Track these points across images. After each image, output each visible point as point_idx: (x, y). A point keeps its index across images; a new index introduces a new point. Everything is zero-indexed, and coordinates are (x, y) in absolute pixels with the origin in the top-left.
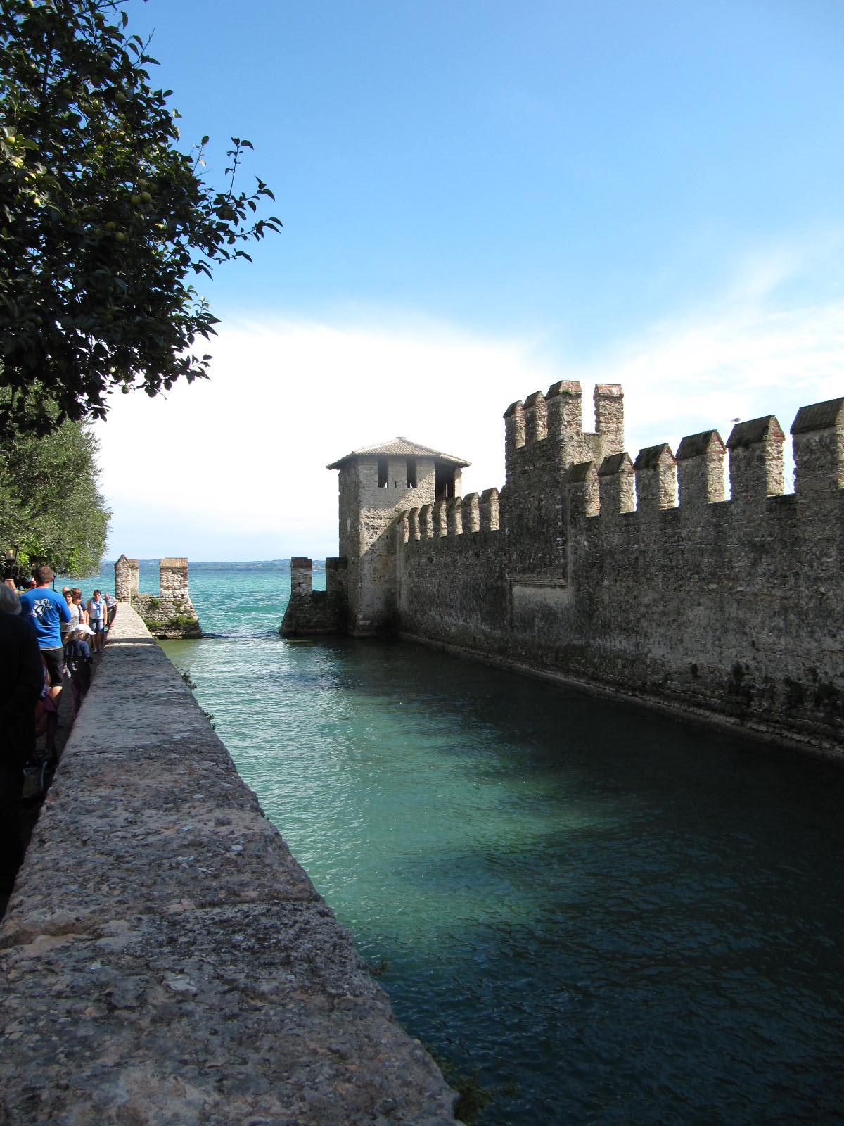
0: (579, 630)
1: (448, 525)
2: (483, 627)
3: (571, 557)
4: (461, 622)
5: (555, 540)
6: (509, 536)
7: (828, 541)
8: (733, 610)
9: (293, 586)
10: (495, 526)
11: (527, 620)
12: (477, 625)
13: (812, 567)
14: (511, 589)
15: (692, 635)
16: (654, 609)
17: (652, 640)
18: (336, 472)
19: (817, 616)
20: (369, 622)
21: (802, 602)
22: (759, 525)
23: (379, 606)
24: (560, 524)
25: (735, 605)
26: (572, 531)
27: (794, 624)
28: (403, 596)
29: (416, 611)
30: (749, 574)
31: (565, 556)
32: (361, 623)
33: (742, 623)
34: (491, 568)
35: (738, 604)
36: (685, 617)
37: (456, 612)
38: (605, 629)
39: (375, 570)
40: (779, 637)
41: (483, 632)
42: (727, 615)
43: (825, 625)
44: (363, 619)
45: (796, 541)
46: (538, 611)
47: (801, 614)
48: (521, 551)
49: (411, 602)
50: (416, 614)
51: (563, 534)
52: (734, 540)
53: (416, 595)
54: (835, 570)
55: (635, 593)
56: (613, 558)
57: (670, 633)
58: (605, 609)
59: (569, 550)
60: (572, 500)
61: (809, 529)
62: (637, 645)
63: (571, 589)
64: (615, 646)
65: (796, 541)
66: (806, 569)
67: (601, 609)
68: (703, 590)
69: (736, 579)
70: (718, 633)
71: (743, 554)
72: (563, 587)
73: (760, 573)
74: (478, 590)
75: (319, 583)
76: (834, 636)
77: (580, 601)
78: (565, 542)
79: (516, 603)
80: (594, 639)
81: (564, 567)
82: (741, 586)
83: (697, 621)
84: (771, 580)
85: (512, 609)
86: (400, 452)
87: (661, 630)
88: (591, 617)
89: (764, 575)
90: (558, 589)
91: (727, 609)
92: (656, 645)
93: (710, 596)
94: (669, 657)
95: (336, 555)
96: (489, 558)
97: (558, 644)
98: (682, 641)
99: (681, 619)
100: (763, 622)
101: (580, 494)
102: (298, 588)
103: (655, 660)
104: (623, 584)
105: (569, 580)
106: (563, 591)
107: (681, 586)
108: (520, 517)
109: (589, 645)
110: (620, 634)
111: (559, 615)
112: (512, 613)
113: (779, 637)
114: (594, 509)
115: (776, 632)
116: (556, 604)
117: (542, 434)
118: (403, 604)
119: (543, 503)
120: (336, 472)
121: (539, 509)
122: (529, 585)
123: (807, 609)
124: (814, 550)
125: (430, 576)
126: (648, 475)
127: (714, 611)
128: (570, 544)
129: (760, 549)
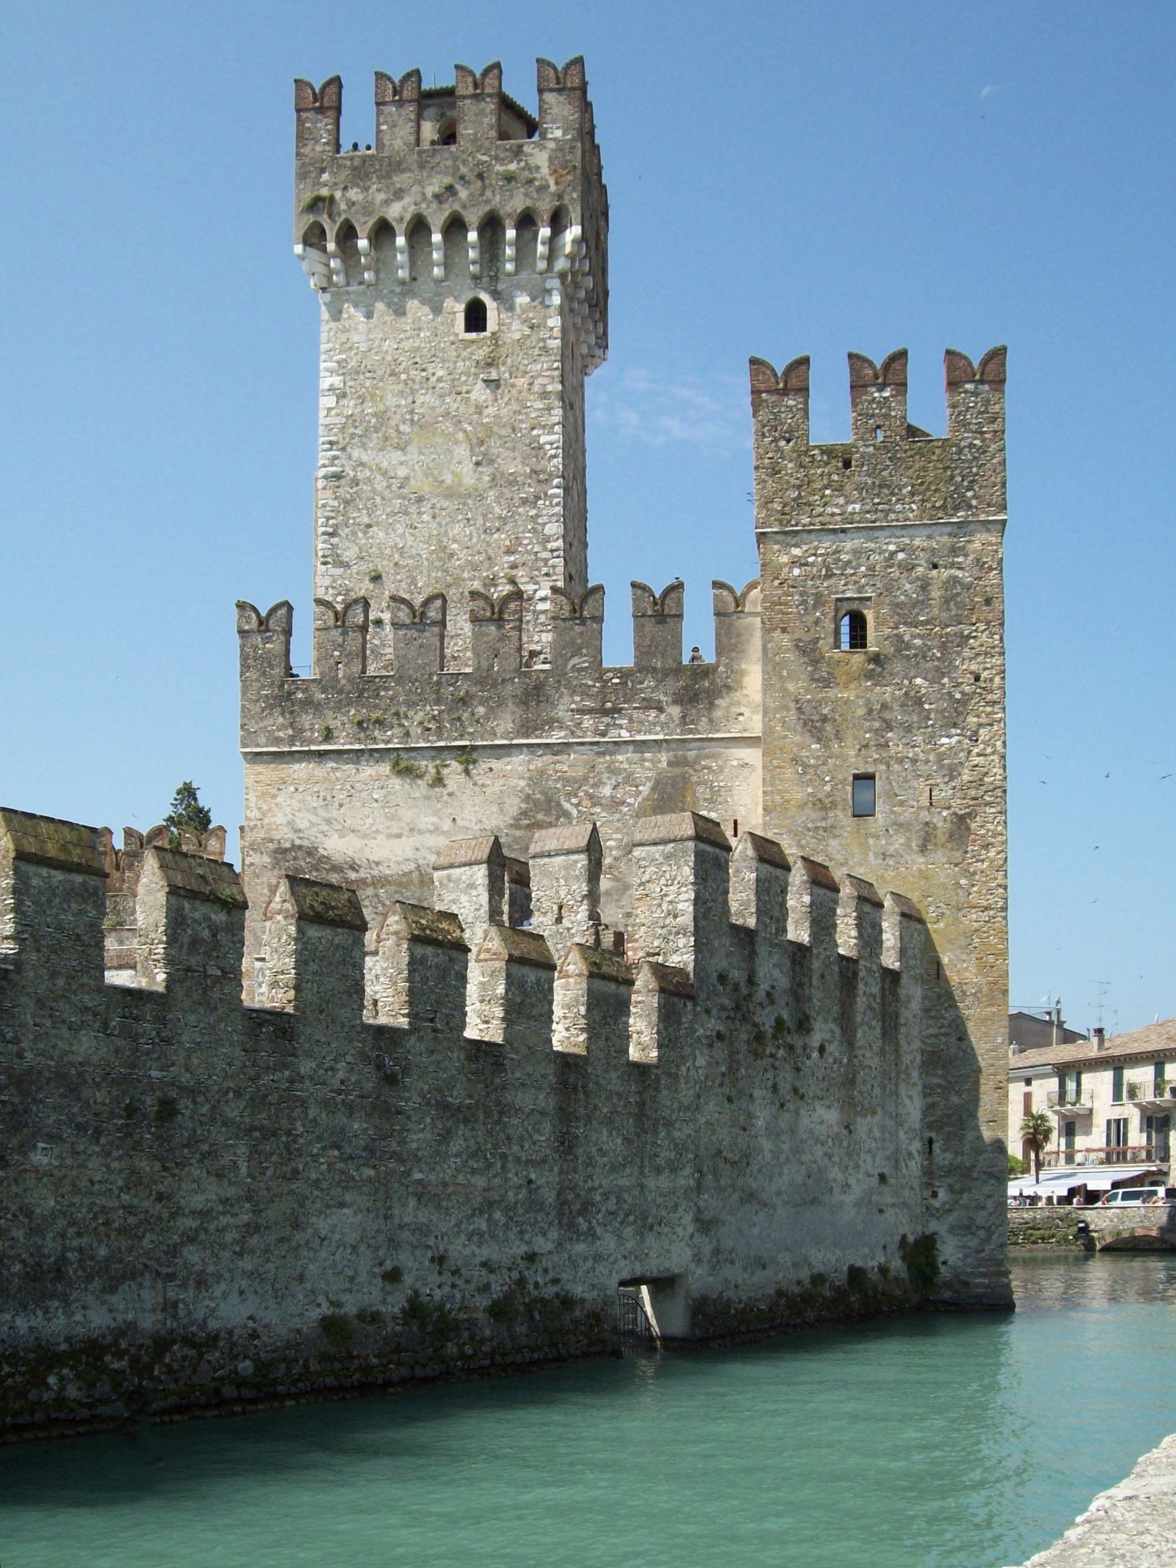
8: (410, 1212)
15: (327, 1264)
17: (218, 1290)
19: (527, 1211)
25: (412, 1202)
33: (422, 1230)
35: (419, 1199)
36: (309, 1231)
42: (397, 1221)
45: (505, 1110)
47: (510, 1209)
54: (548, 1151)
56: (73, 1091)
57: (270, 1266)
62: (170, 1307)
65: (505, 1110)
66: (516, 1148)
70: (381, 1253)
73: (454, 1151)
82: (421, 1171)
83: (337, 1236)
84: (471, 1163)
87: (247, 1264)
91: (396, 1211)
92: (234, 1298)
93: (364, 1189)
98: (301, 1278)
99: (299, 1237)
100: (459, 1225)
123: (516, 1203)
127: (372, 1216)
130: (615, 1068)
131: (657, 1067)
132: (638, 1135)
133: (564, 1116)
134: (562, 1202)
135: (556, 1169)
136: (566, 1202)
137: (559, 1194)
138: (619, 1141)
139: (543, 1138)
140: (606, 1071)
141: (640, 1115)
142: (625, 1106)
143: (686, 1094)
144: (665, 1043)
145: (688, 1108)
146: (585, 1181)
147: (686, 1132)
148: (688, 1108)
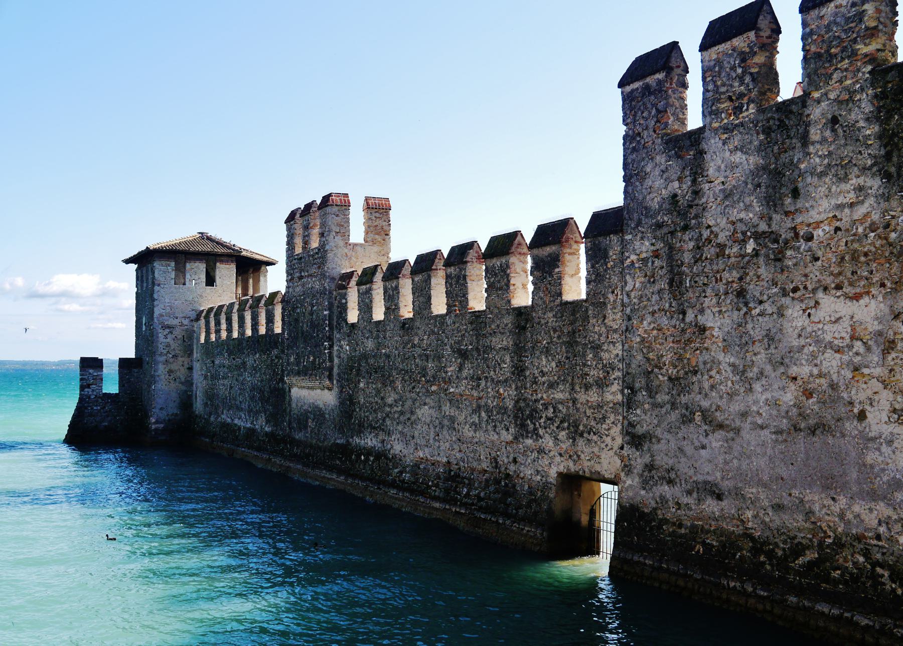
0: (341, 430)
1: (240, 327)
2: (266, 429)
3: (336, 360)
4: (249, 425)
5: (323, 344)
6: (288, 339)
7: (505, 349)
8: (447, 409)
9: (82, 388)
10: (278, 329)
11: (302, 420)
12: (262, 424)
13: (495, 372)
14: (290, 391)
16: (395, 408)
18: (134, 267)
19: (498, 413)
20: (162, 426)
21: (489, 401)
22: (464, 335)
23: (173, 409)
24: (327, 329)
25: (448, 404)
26: (338, 336)
27: (485, 420)
28: (198, 399)
29: (210, 414)
30: (457, 377)
31: (331, 360)
32: (153, 427)
33: (452, 419)
34: (274, 370)
37: (245, 415)
38: (360, 429)
39: (170, 372)
40: (475, 431)
41: (266, 434)
43: (503, 420)
44: (157, 422)
46: (310, 412)
48: (297, 354)
49: (206, 405)
50: (210, 417)
51: (330, 339)
52: (448, 347)
53: (211, 396)
55: (382, 395)
58: (360, 410)
59: (335, 353)
60: (338, 307)
61: (494, 340)
63: (336, 390)
64: (367, 443)
66: (492, 373)
67: (358, 410)
68: (428, 391)
69: (449, 381)
71: (454, 360)
72: (330, 389)
74: (263, 393)
75: (111, 386)
76: (508, 430)
77: (342, 403)
78: (331, 346)
79: (294, 405)
80: (352, 437)
81: (331, 369)
83: (424, 419)
85: (290, 411)
86: (199, 248)
87: (400, 428)
88: (350, 417)
89: (466, 378)
90: (326, 391)
91: (443, 408)
92: (396, 442)
94: (405, 452)
95: (131, 354)
96: (272, 360)
97: (326, 443)
98: (413, 437)
99: (413, 418)
101: (344, 301)
102: (86, 390)
103: (395, 455)
104: (374, 386)
105: (335, 382)
106: (330, 393)
107: (414, 388)
108: (297, 320)
109: (348, 443)
110: (371, 432)
111: (327, 416)
112: (290, 415)
113: (475, 431)
114: (353, 316)
115: (474, 427)
116: (325, 405)
117: (315, 244)
118: (199, 406)
119: (315, 308)
120: (134, 267)
121: (311, 314)
122: (304, 387)
124: (496, 357)
125: (224, 378)
126: (392, 286)
128: (336, 348)
129: (463, 355)
130: (551, 310)
131: (586, 301)
132: (567, 358)
133: (519, 351)
134: (518, 409)
135: (513, 386)
136: (520, 409)
137: (517, 402)
138: (554, 364)
139: (505, 366)
140: (544, 314)
141: (571, 344)
142: (559, 337)
143: (615, 319)
144: (595, 279)
145: (615, 331)
146: (532, 395)
147: (615, 352)
148: (615, 331)
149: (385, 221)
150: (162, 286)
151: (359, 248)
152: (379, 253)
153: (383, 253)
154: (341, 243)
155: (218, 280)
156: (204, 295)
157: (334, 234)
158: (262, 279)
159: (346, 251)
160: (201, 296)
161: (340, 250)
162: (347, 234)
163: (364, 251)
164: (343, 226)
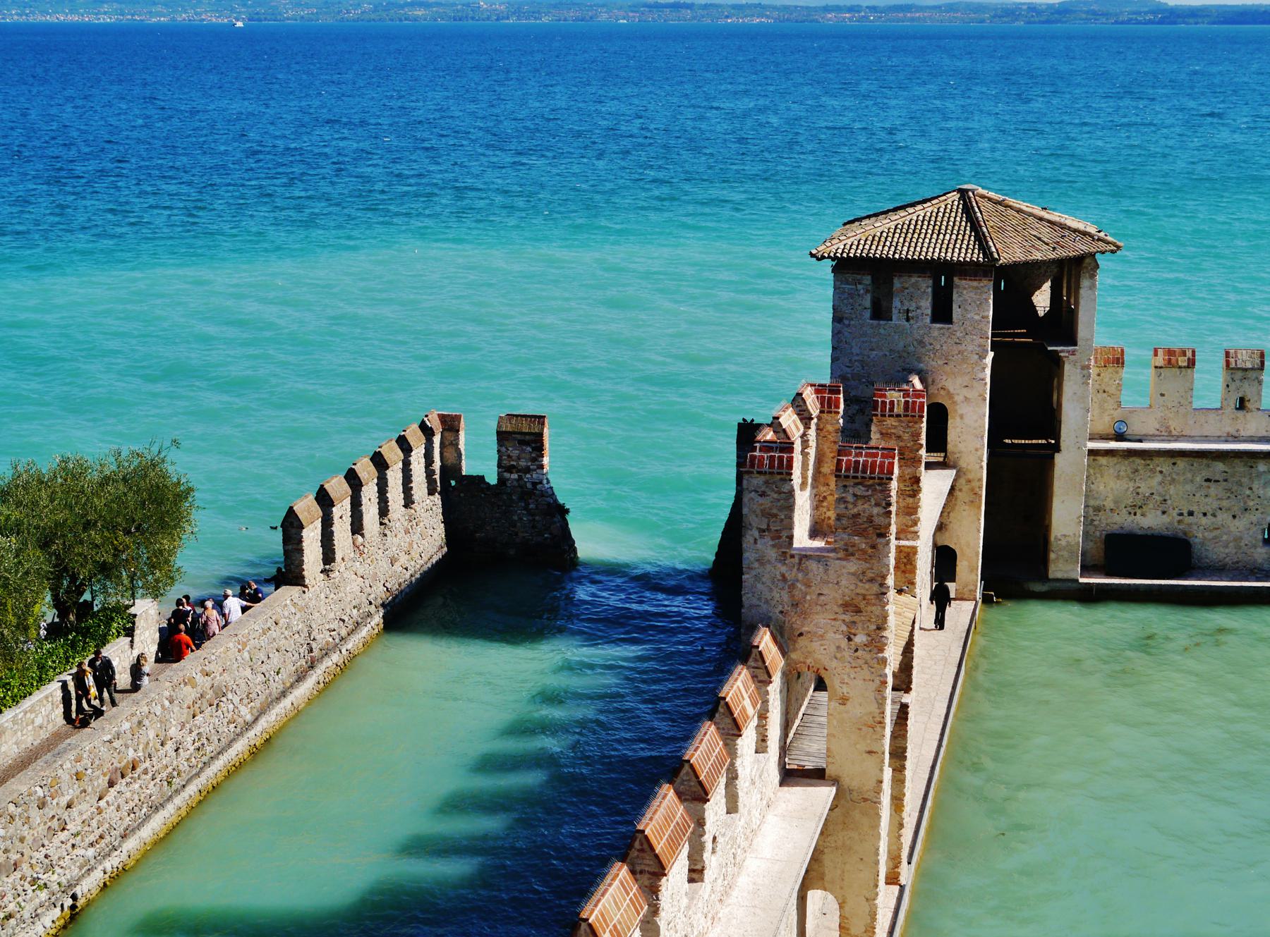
149: (877, 505)
150: (846, 322)
151: (812, 565)
152: (860, 576)
153: (870, 574)
154: (772, 554)
155: (956, 313)
156: (926, 339)
157: (756, 534)
158: (1085, 283)
159: (784, 569)
160: (921, 343)
161: (769, 567)
162: (784, 534)
163: (826, 571)
164: (775, 516)
